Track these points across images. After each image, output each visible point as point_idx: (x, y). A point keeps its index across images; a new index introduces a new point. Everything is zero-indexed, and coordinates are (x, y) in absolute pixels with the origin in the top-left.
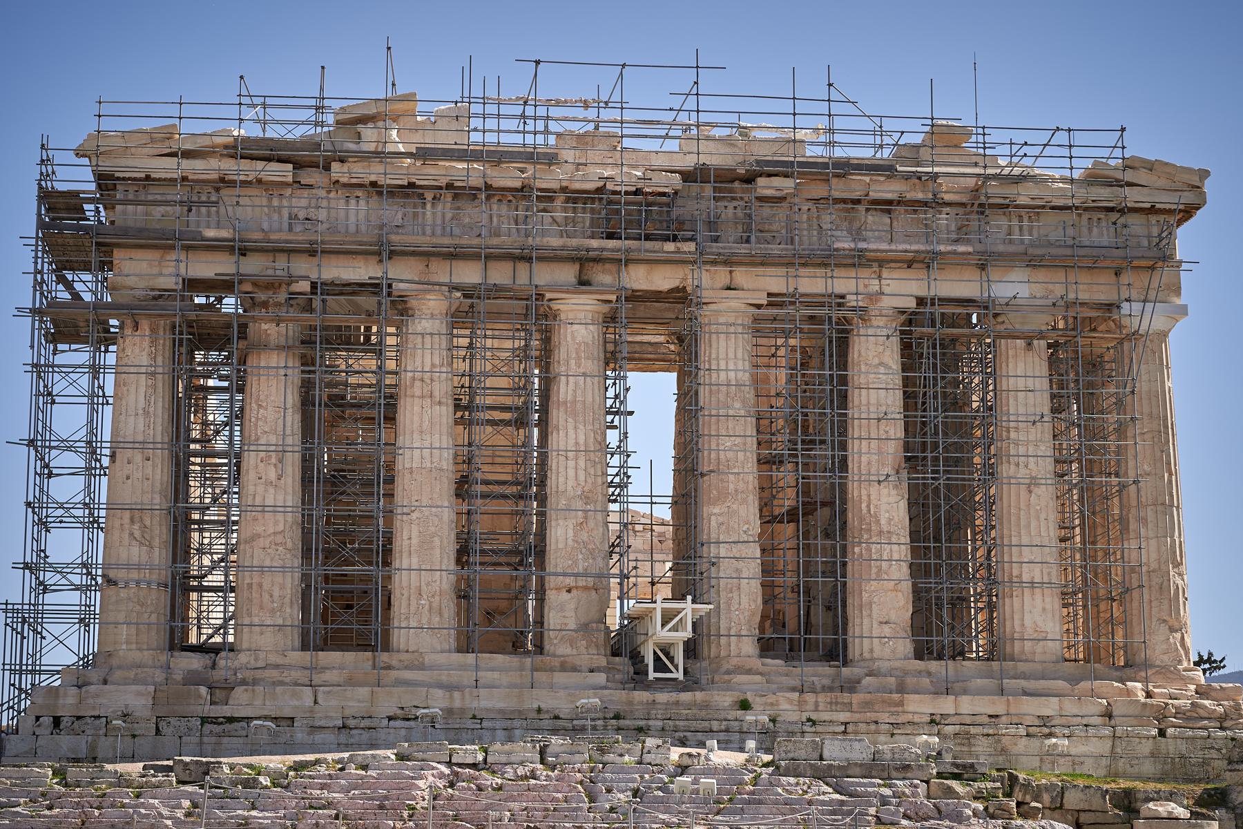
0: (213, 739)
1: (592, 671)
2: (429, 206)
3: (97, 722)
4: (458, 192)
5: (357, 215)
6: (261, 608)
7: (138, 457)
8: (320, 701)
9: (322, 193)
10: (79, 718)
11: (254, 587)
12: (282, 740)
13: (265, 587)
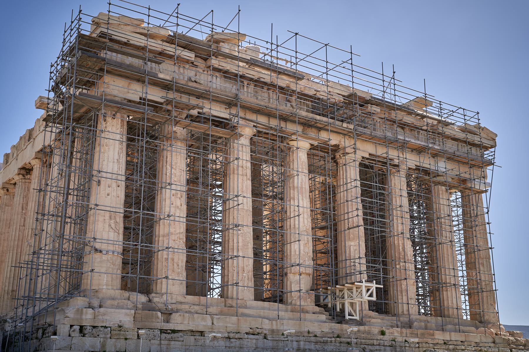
0: (166, 342)
1: (314, 313)
2: (245, 88)
3: (106, 330)
4: (258, 83)
5: (218, 84)
6: (173, 271)
7: (114, 185)
8: (215, 323)
9: (201, 71)
10: (94, 327)
11: (169, 260)
12: (200, 343)
13: (175, 261)
